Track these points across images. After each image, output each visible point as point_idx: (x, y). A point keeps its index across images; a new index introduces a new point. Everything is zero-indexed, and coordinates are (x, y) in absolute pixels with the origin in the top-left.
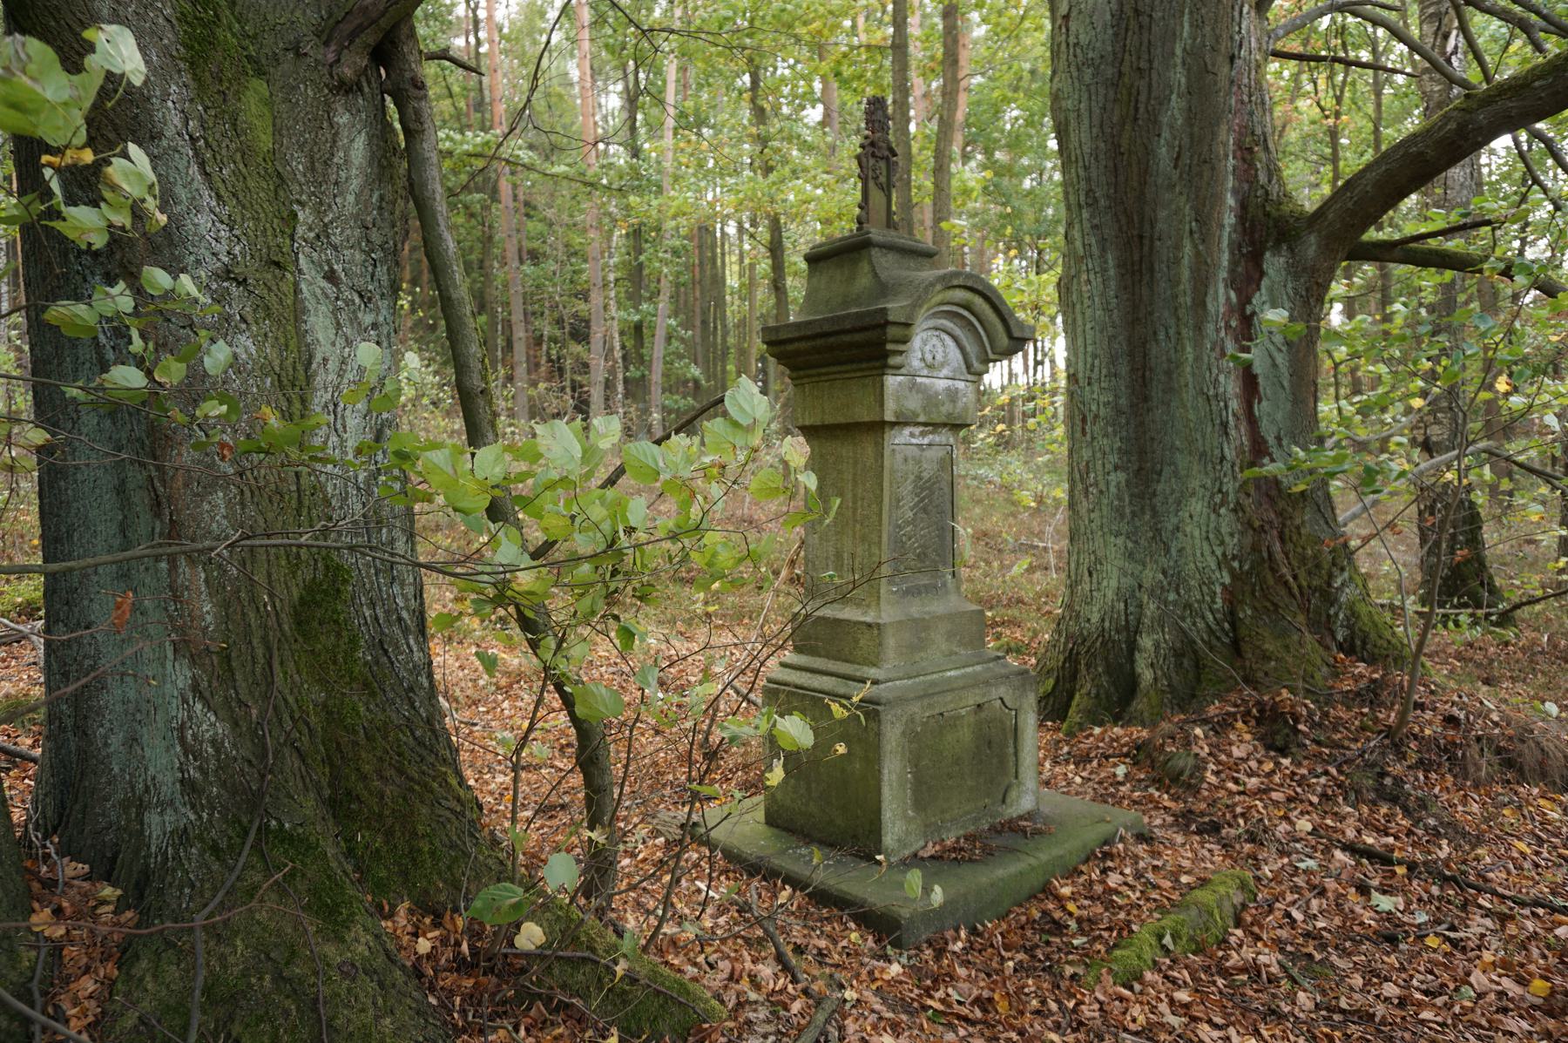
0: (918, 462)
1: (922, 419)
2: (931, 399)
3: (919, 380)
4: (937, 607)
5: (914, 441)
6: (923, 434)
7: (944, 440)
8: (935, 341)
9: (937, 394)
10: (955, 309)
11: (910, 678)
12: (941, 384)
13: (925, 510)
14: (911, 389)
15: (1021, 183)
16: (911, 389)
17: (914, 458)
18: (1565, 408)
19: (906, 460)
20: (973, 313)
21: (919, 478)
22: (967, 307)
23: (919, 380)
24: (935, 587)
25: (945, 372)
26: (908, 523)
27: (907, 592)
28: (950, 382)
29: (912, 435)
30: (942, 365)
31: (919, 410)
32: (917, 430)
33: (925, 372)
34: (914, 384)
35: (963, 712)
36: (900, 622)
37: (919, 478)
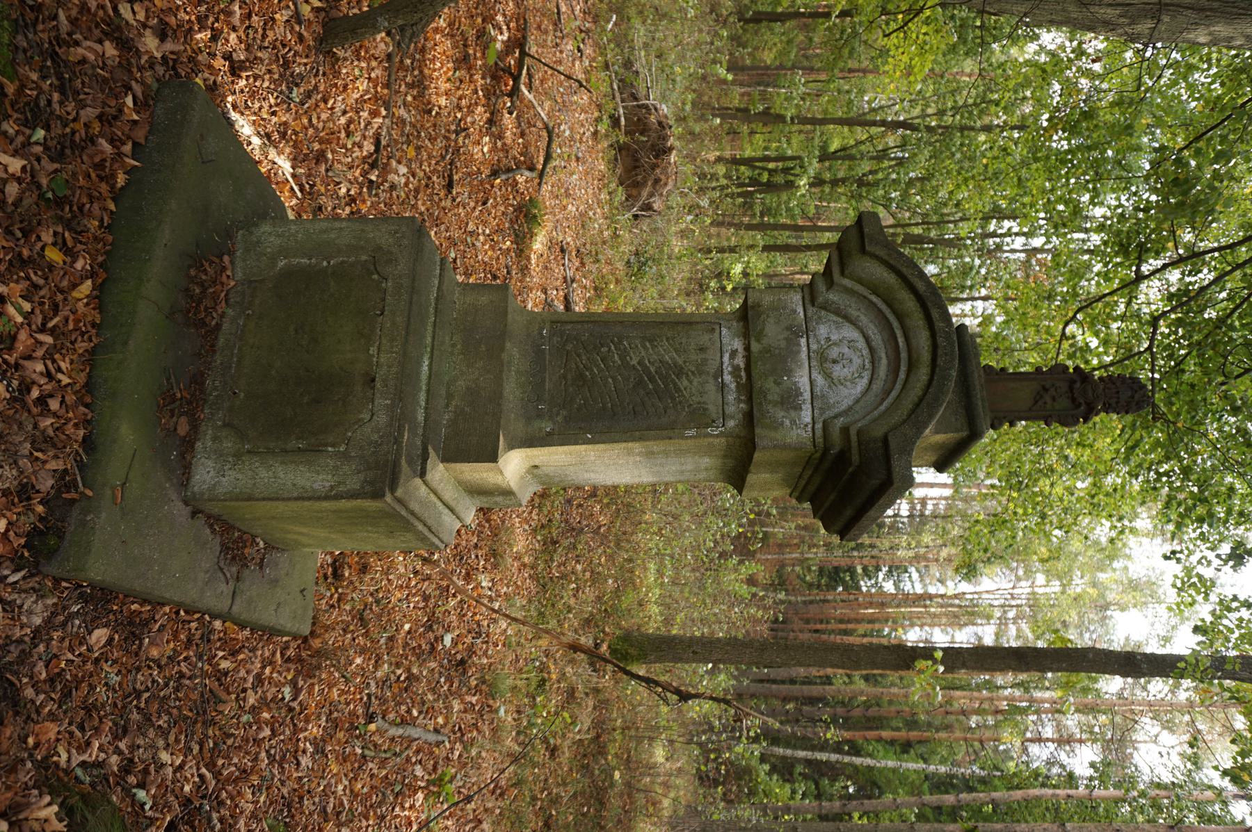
0: (700, 371)
1: (755, 347)
2: (782, 361)
3: (803, 341)
4: (512, 390)
5: (726, 358)
6: (735, 371)
7: (731, 409)
8: (857, 361)
9: (789, 373)
10: (904, 355)
11: (437, 299)
12: (802, 380)
13: (640, 382)
14: (789, 328)
15: (1045, 63)
16: (789, 328)
17: (705, 361)
18: (795, 829)
19: (702, 349)
20: (889, 305)
21: (680, 372)
22: (911, 366)
23: (803, 341)
24: (539, 399)
25: (820, 380)
26: (624, 355)
27: (539, 353)
28: (807, 395)
29: (733, 354)
30: (828, 376)
31: (765, 341)
32: (740, 361)
33: (814, 347)
34: (798, 336)
35: (373, 350)
36: (505, 313)
37: (680, 372)
